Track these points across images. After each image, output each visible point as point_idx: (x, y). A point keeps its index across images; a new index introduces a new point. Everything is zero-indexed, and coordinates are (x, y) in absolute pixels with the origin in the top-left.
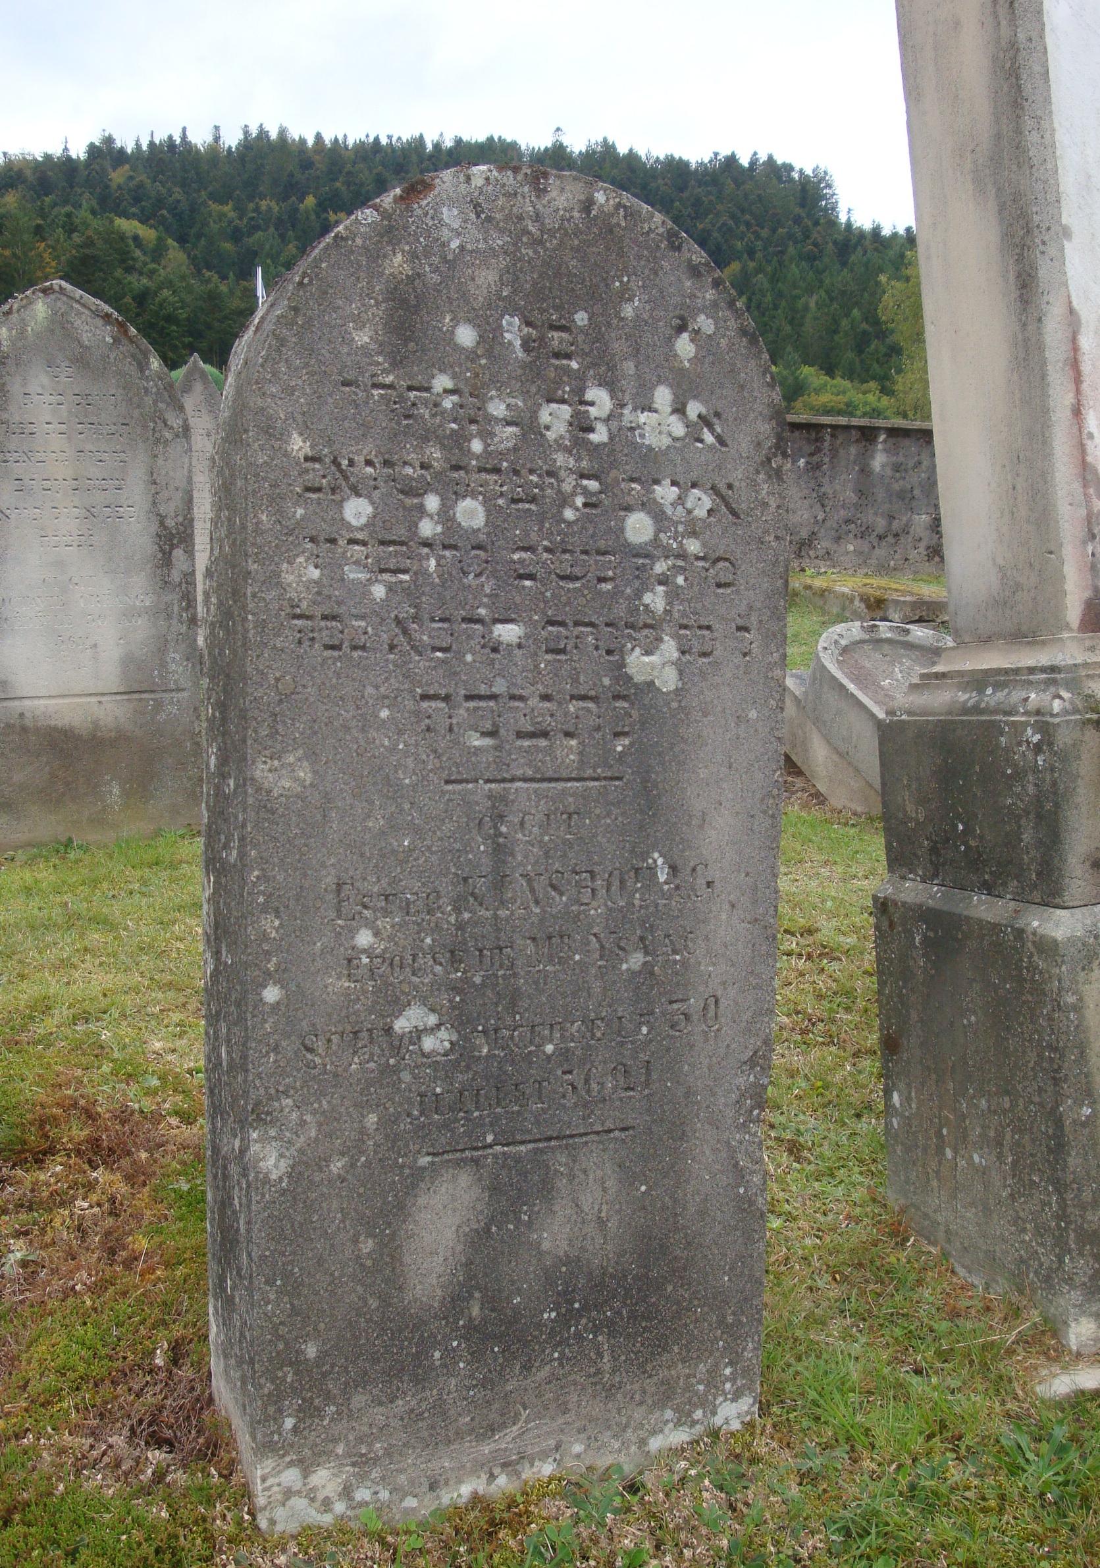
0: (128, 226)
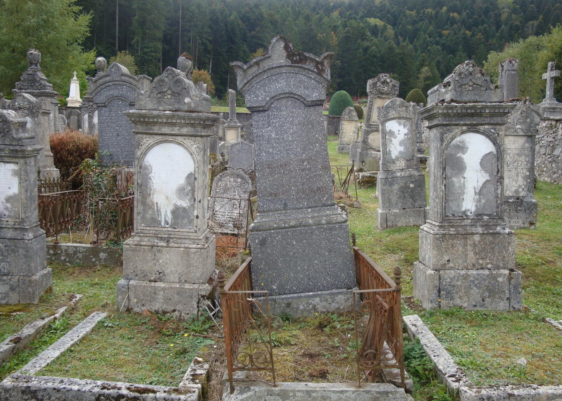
0: (373, 21)
